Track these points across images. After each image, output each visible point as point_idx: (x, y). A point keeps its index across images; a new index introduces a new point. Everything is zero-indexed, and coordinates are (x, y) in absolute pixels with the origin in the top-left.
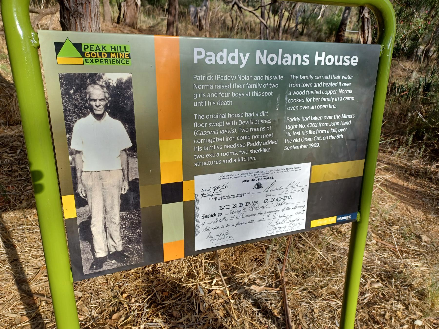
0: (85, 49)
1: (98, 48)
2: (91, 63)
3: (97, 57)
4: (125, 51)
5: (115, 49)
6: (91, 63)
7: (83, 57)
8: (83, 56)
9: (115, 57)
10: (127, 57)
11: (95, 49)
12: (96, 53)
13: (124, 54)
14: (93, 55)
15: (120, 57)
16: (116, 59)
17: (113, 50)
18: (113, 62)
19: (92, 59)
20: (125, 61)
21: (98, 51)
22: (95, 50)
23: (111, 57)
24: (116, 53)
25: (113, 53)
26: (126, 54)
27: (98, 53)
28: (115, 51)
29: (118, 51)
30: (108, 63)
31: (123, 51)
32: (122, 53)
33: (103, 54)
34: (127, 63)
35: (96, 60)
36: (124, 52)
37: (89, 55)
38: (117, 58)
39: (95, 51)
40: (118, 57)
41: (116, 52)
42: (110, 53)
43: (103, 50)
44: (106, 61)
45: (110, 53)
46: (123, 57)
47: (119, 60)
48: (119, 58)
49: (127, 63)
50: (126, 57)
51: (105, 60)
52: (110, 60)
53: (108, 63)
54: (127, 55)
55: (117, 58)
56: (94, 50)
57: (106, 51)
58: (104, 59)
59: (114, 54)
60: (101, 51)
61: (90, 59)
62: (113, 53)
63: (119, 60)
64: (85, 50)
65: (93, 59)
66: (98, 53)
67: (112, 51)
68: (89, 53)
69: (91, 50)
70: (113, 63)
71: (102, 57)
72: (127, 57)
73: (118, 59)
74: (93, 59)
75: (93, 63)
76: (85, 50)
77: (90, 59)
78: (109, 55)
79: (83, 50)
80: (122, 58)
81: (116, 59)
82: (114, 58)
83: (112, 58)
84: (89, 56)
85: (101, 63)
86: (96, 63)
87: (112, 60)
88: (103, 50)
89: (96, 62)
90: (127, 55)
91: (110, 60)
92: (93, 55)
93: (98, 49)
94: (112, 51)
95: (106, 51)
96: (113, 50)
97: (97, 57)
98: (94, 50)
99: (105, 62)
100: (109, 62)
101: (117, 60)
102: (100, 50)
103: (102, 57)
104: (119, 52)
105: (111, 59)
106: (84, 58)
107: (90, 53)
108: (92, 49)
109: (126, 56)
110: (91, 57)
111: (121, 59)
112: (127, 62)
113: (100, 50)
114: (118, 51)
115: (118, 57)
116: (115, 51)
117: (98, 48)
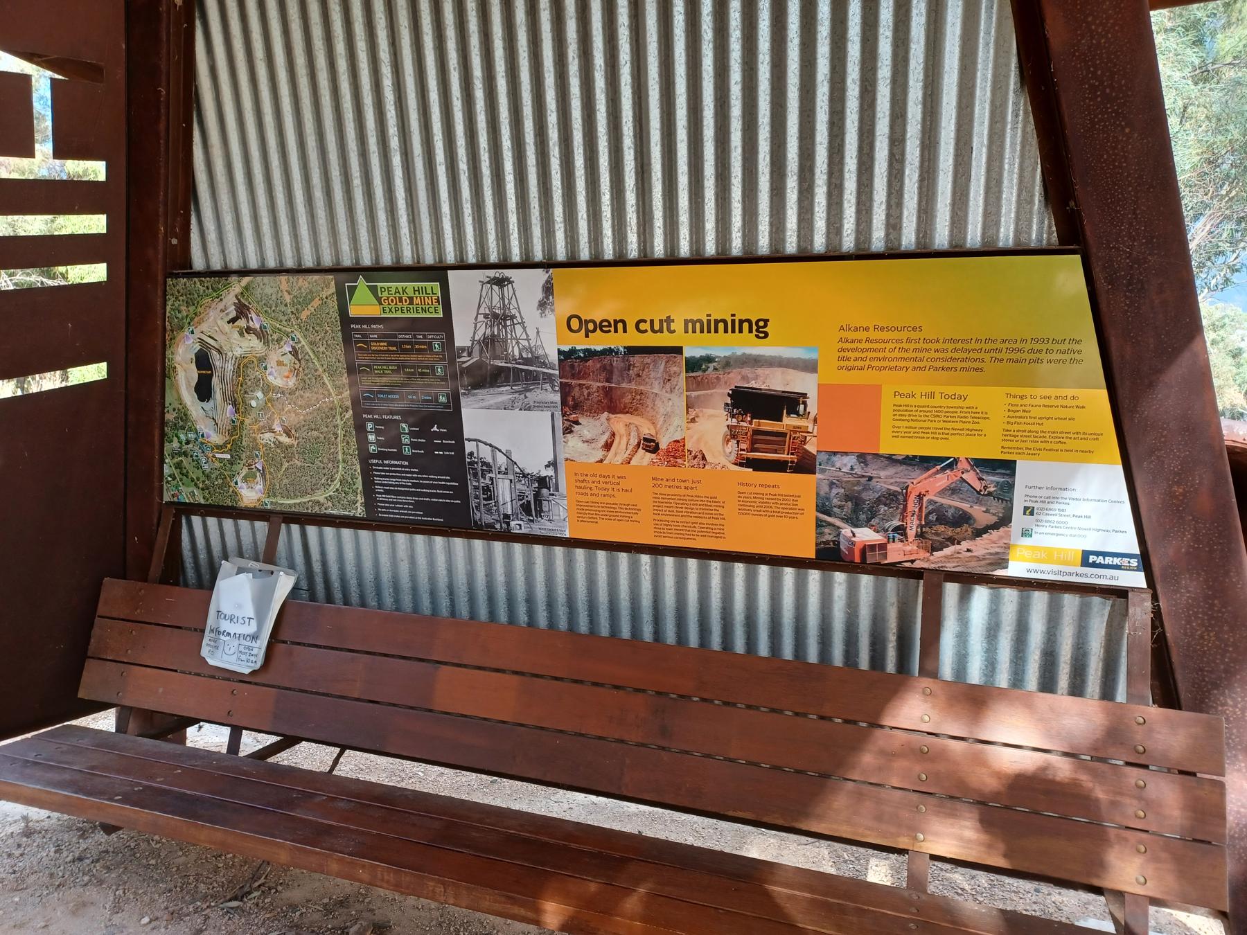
0: (382, 292)
3: (396, 304)
5: (419, 291)
12: (395, 298)
14: (392, 301)
17: (417, 293)
73: (424, 307)
78: (411, 299)
79: (380, 295)
92: (392, 301)
96: (417, 293)
97: (396, 304)
100: (412, 311)
104: (424, 295)
105: (415, 307)
107: (388, 298)
109: (434, 301)
111: (427, 307)
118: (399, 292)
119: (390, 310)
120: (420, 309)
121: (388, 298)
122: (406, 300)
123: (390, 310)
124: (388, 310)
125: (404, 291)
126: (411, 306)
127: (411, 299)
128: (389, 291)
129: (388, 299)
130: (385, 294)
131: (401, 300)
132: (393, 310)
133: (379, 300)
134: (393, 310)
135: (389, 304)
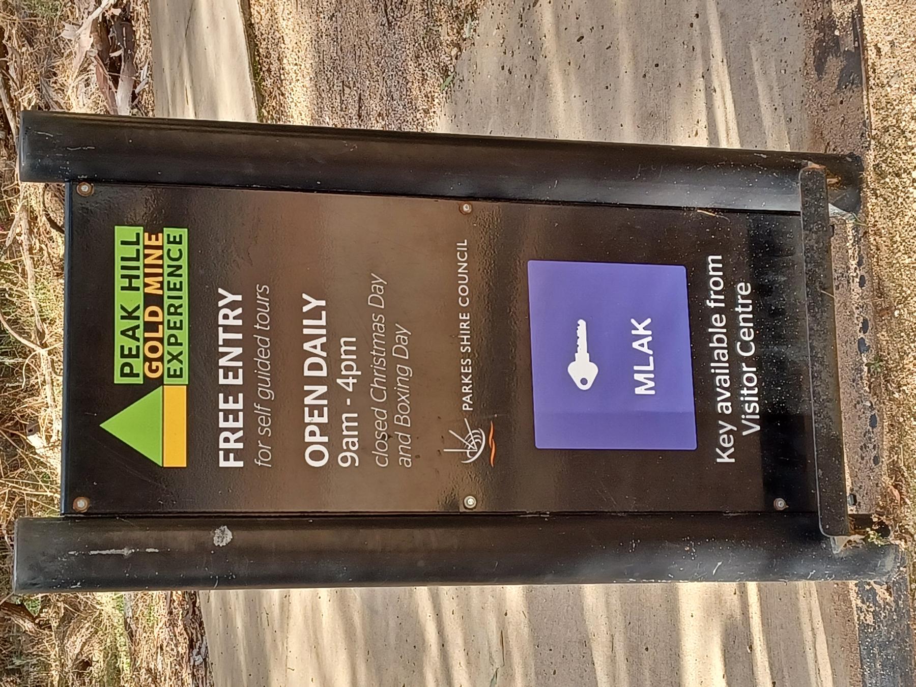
0: (132, 374)
1: (130, 333)
2: (181, 362)
3: (161, 340)
4: (137, 243)
5: (130, 277)
6: (181, 362)
7: (163, 385)
8: (160, 382)
9: (160, 279)
10: (157, 239)
11: (133, 344)
12: (146, 340)
13: (146, 247)
14: (154, 349)
15: (160, 262)
16: (167, 279)
17: (135, 283)
18: (175, 289)
19: (167, 357)
20: (171, 246)
21: (139, 333)
22: (138, 344)
23: (160, 292)
24: (146, 275)
25: (146, 285)
26: (147, 243)
27: (147, 335)
28: (138, 277)
29: (138, 268)
30: (181, 306)
31: (138, 251)
32: (146, 256)
33: (148, 319)
34: (180, 243)
35: (169, 344)
36: (141, 247)
37: (154, 364)
38: (162, 275)
39: (141, 344)
40: (160, 271)
41: (140, 273)
42: (146, 295)
43: (138, 318)
44: (172, 310)
45: (146, 295)
46: (158, 253)
47: (169, 266)
48: (161, 266)
49: (180, 243)
50: (159, 243)
51: (169, 314)
52: (169, 297)
53: (181, 306)
54: (150, 239)
55: (162, 275)
56: (138, 347)
57: (138, 307)
58: (167, 317)
59: (148, 280)
60: (140, 322)
61: (169, 362)
62: (146, 285)
63: (169, 266)
64: (137, 375)
65: (169, 353)
66: (147, 335)
67: (138, 289)
68: (147, 364)
69: (137, 356)
70: (180, 289)
71: (162, 323)
72: (157, 239)
73: (167, 270)
74: (169, 353)
75: (181, 353)
76: (137, 375)
77: (169, 362)
78: (150, 300)
79: (140, 381)
80: (161, 258)
81: (167, 279)
82: (162, 283)
83: (162, 288)
84: (159, 364)
85: (181, 328)
86: (181, 344)
87: (169, 289)
88: (138, 318)
89: (177, 344)
90: (150, 239)
91: (169, 297)
92: (154, 349)
93: (134, 333)
94: (138, 289)
95: (138, 307)
96: (135, 283)
97: (161, 340)
98: (138, 347)
99: (176, 313)
100: (177, 302)
101: (170, 275)
102: (138, 327)
103: (162, 323)
104: (140, 264)
105: (167, 293)
106: (166, 380)
107: (146, 359)
108: (134, 352)
109: (153, 242)
110: (161, 359)
111: (167, 262)
112: (174, 242)
113: (138, 327)
114: (138, 268)
115: (160, 271)
116: (138, 277)
117: (130, 333)
119: (175, 357)
120: (173, 280)
121: (146, 359)
123: (175, 357)
124: (175, 365)
125: (130, 316)
126: (167, 302)
127: (150, 300)
128: (130, 355)
129: (151, 360)
130: (138, 365)
131: (151, 327)
132: (175, 350)
133: (151, 385)
134: (175, 350)
135: (161, 359)
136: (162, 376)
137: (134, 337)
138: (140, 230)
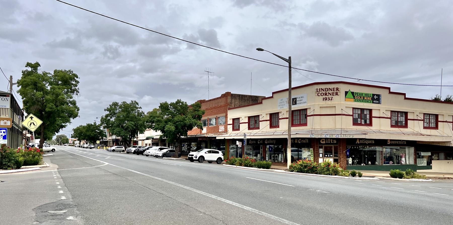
0: (355, 94)
3: (359, 99)
5: (366, 95)
12: (359, 97)
17: (366, 95)
33: (362, 97)
78: (364, 97)
79: (354, 95)
96: (366, 95)
97: (359, 99)
100: (364, 101)
106: (355, 99)
107: (357, 96)
109: (370, 99)
110: (357, 99)
111: (368, 100)
118: (360, 95)
119: (357, 101)
120: (366, 101)
122: (362, 98)
123: (357, 101)
126: (364, 100)
128: (357, 94)
129: (357, 97)
131: (361, 97)
135: (357, 99)
136: (355, 99)
137: (359, 95)
138: (372, 97)
